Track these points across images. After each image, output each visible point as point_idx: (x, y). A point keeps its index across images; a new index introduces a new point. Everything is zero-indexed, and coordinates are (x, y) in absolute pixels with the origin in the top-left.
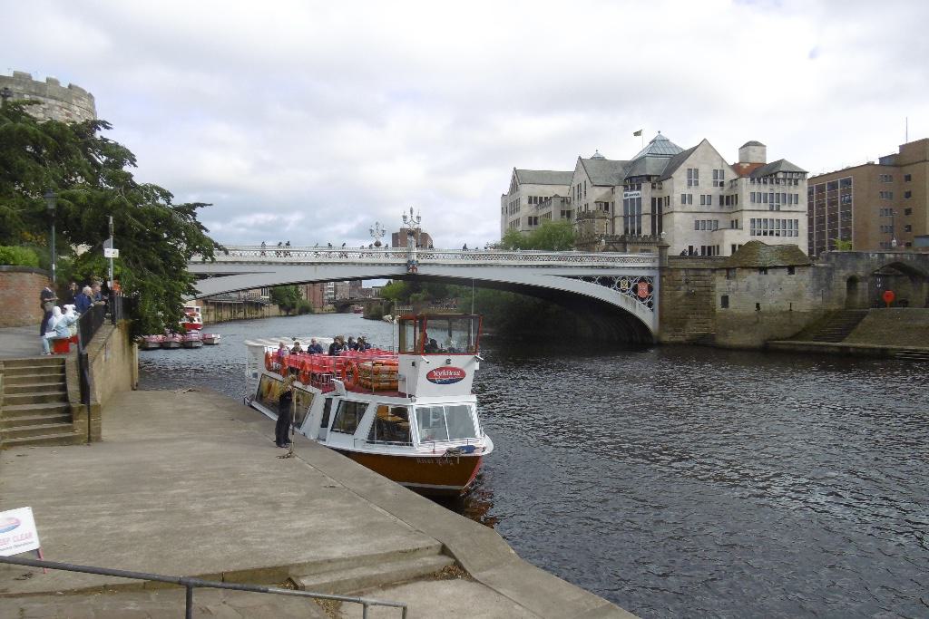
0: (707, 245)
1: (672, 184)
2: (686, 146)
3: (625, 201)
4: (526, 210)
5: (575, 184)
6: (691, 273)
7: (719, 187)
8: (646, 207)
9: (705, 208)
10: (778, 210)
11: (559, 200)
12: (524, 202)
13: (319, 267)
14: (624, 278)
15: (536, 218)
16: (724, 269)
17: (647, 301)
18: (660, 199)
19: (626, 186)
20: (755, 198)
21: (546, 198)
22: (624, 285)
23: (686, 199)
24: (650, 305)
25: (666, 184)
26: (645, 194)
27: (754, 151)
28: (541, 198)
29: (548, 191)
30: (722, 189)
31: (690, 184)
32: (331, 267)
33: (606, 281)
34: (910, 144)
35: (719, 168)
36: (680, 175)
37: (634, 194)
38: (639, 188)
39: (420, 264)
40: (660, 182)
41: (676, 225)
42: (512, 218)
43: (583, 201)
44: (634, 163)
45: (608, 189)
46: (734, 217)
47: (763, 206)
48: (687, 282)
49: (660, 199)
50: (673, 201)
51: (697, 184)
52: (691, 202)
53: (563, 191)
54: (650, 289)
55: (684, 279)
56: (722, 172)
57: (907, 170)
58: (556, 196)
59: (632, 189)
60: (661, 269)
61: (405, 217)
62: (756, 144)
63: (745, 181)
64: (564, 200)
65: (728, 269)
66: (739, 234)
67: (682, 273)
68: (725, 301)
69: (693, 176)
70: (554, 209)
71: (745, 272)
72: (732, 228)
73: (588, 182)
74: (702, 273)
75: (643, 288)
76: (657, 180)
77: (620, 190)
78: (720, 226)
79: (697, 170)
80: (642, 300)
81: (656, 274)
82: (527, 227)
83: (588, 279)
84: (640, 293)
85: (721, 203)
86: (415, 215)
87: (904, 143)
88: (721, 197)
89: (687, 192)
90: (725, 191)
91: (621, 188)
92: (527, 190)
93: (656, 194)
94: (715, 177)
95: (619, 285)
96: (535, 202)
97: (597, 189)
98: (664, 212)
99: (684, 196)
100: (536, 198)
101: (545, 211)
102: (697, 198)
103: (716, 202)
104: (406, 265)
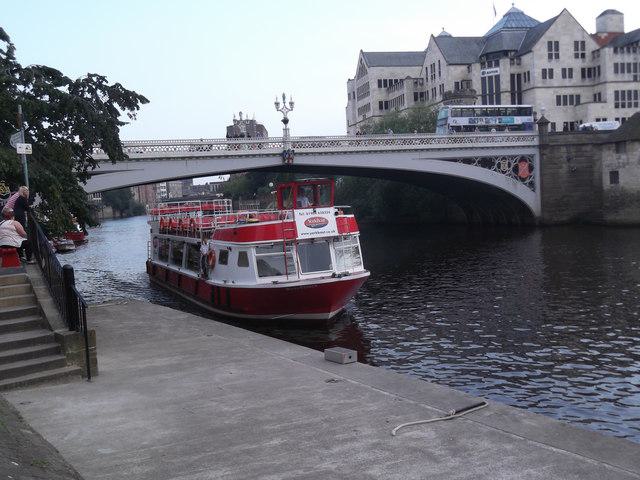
0: (569, 121)
2: (542, 18)
3: (483, 79)
4: (377, 95)
5: (427, 64)
6: (573, 150)
7: (580, 60)
8: (505, 85)
9: (567, 82)
11: (411, 82)
12: (374, 86)
13: (190, 162)
14: (504, 158)
15: (386, 102)
16: (611, 143)
17: (527, 181)
19: (483, 64)
20: (619, 68)
21: (396, 81)
22: (504, 166)
23: (547, 74)
24: (531, 185)
25: (525, 59)
26: (504, 70)
27: (612, 20)
28: (391, 81)
29: (399, 72)
30: (583, 62)
31: (550, 56)
32: (199, 162)
33: (486, 163)
35: (580, 39)
36: (541, 48)
37: (491, 71)
38: (497, 65)
39: (295, 154)
41: (538, 102)
42: (361, 103)
43: (438, 82)
44: (487, 39)
45: (464, 68)
46: (597, 89)
47: (628, 76)
48: (569, 160)
49: (519, 75)
50: (534, 77)
51: (557, 56)
52: (551, 77)
53: (414, 72)
54: (531, 168)
55: (565, 156)
56: (583, 43)
58: (408, 78)
59: (490, 66)
60: (542, 147)
61: (277, 104)
62: (613, 12)
63: (608, 51)
64: (417, 82)
65: (618, 143)
66: (603, 107)
67: (564, 149)
68: (614, 176)
69: (554, 49)
70: (407, 91)
71: (637, 145)
72: (595, 101)
73: (443, 61)
74: (584, 148)
75: (523, 168)
76: (517, 56)
77: (476, 68)
78: (582, 100)
79: (557, 43)
80: (523, 180)
81: (535, 152)
82: (377, 112)
83: (468, 161)
84: (520, 173)
85: (583, 76)
86: (288, 101)
88: (583, 70)
89: (548, 66)
90: (587, 63)
91: (478, 66)
92: (375, 74)
93: (515, 70)
94: (576, 48)
95: (499, 166)
96: (385, 86)
97: (452, 68)
98: (524, 88)
99: (544, 71)
100: (385, 81)
101: (396, 94)
102: (558, 72)
103: (577, 75)
104: (281, 155)
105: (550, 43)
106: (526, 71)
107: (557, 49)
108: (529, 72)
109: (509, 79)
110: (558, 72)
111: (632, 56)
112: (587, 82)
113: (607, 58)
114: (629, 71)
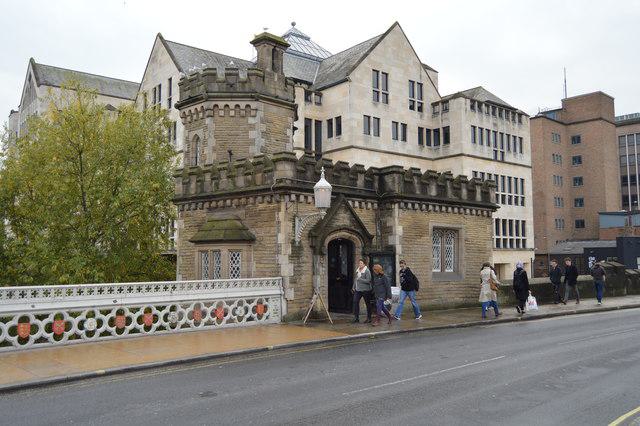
7: (416, 113)
9: (399, 146)
10: (503, 161)
18: (318, 123)
25: (332, 96)
30: (421, 117)
34: (570, 99)
35: (417, 80)
36: (362, 79)
40: (319, 93)
47: (488, 152)
49: (318, 123)
57: (575, 130)
85: (421, 142)
88: (420, 130)
90: (427, 122)
102: (386, 126)
103: (413, 136)
106: (333, 117)
108: (339, 119)
110: (386, 126)
111: (491, 119)
112: (426, 152)
113: (463, 118)
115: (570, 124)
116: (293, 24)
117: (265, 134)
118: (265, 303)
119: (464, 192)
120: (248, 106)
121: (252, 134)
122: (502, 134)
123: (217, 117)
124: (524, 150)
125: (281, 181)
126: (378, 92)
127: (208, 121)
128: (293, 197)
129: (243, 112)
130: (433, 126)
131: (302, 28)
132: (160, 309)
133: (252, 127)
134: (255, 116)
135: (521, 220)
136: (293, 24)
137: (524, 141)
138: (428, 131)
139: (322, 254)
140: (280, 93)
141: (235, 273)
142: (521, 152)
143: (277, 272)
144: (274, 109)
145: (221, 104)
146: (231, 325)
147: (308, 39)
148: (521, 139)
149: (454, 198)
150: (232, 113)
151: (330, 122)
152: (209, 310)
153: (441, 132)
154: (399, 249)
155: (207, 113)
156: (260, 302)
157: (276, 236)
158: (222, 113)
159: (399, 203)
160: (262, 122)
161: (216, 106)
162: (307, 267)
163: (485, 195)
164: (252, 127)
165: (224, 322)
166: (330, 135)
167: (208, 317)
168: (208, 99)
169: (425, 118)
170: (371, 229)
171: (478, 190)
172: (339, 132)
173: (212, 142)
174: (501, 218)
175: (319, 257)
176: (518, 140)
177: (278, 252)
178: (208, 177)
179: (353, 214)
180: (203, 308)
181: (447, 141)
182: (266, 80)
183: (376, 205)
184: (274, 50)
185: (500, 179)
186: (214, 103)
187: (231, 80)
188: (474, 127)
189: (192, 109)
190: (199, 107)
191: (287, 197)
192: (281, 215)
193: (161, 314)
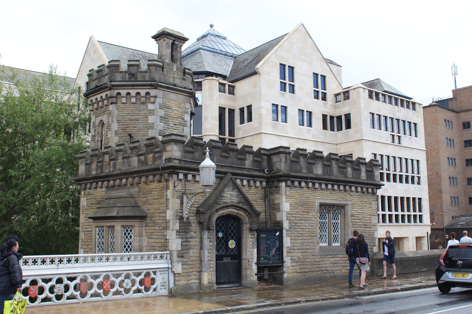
1: (255, 86)
18: (232, 111)
30: (325, 106)
31: (283, 87)
35: (320, 73)
47: (385, 136)
49: (232, 111)
50: (260, 116)
79: (292, 68)
85: (325, 127)
87: (454, 88)
88: (324, 117)
102: (293, 114)
103: (317, 122)
105: (283, 66)
106: (245, 105)
107: (292, 79)
108: (249, 107)
109: (216, 114)
110: (293, 114)
113: (362, 105)
114: (386, 130)
115: (461, 112)
116: (211, 26)
117: (164, 119)
118: (152, 276)
119: (349, 170)
120: (148, 93)
121: (151, 119)
122: (398, 120)
123: (119, 104)
124: (418, 134)
125: (169, 160)
126: (285, 84)
127: (111, 107)
128: (181, 176)
129: (143, 99)
130: (336, 113)
131: (218, 29)
132: (46, 281)
133: (152, 112)
134: (154, 103)
135: (417, 197)
136: (211, 26)
137: (418, 126)
138: (332, 118)
139: (209, 229)
140: (177, 82)
141: (128, 248)
142: (416, 136)
143: (165, 247)
144: (172, 96)
145: (123, 92)
146: (118, 297)
147: (225, 38)
148: (415, 124)
149: (341, 178)
150: (133, 100)
151: (242, 110)
152: (96, 282)
153: (343, 118)
154: (286, 225)
155: (111, 100)
156: (148, 274)
157: (165, 212)
158: (124, 100)
159: (286, 181)
160: (161, 107)
161: (119, 94)
162: (194, 242)
163: (370, 173)
164: (152, 112)
165: (111, 294)
166: (242, 122)
167: (95, 289)
168: (111, 88)
169: (329, 106)
170: (259, 207)
171: (363, 169)
172: (250, 119)
173: (115, 126)
174: (386, 195)
175: (206, 232)
176: (413, 125)
177: (166, 228)
178: (107, 158)
179: (240, 191)
180: (90, 280)
181: (348, 126)
182: (165, 70)
183: (264, 184)
184: (173, 44)
185: (385, 159)
186: (117, 91)
187: (133, 70)
188: (373, 114)
189: (98, 97)
190: (104, 95)
191: (175, 177)
192: (169, 193)
193: (47, 286)
